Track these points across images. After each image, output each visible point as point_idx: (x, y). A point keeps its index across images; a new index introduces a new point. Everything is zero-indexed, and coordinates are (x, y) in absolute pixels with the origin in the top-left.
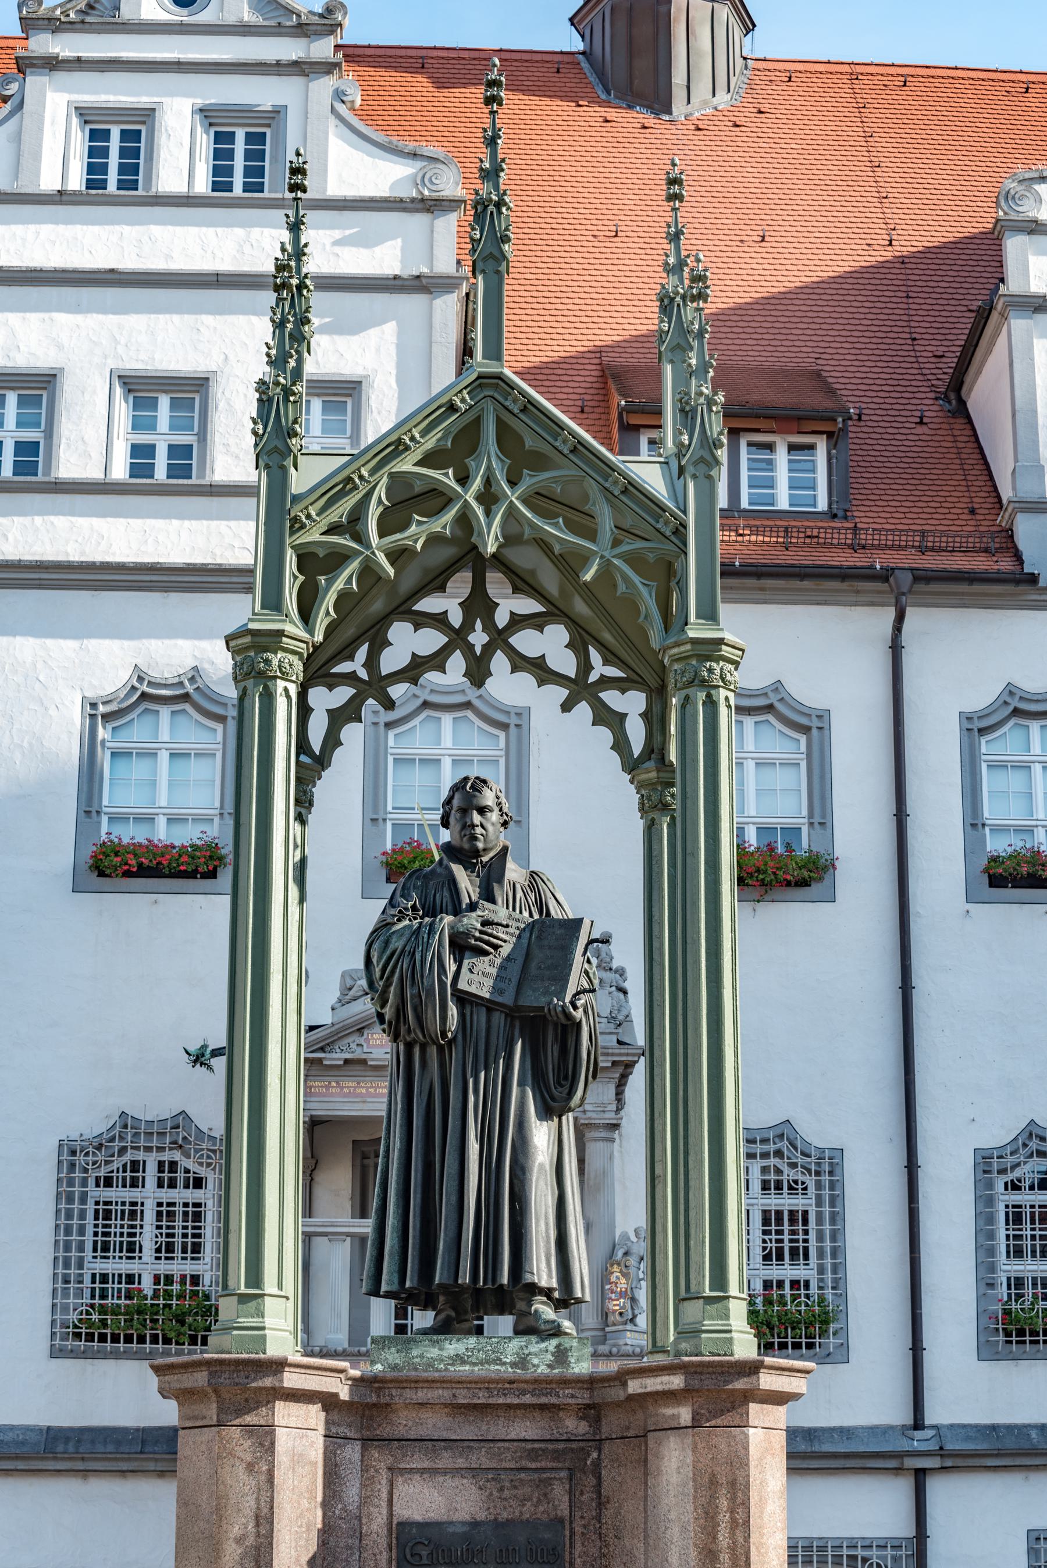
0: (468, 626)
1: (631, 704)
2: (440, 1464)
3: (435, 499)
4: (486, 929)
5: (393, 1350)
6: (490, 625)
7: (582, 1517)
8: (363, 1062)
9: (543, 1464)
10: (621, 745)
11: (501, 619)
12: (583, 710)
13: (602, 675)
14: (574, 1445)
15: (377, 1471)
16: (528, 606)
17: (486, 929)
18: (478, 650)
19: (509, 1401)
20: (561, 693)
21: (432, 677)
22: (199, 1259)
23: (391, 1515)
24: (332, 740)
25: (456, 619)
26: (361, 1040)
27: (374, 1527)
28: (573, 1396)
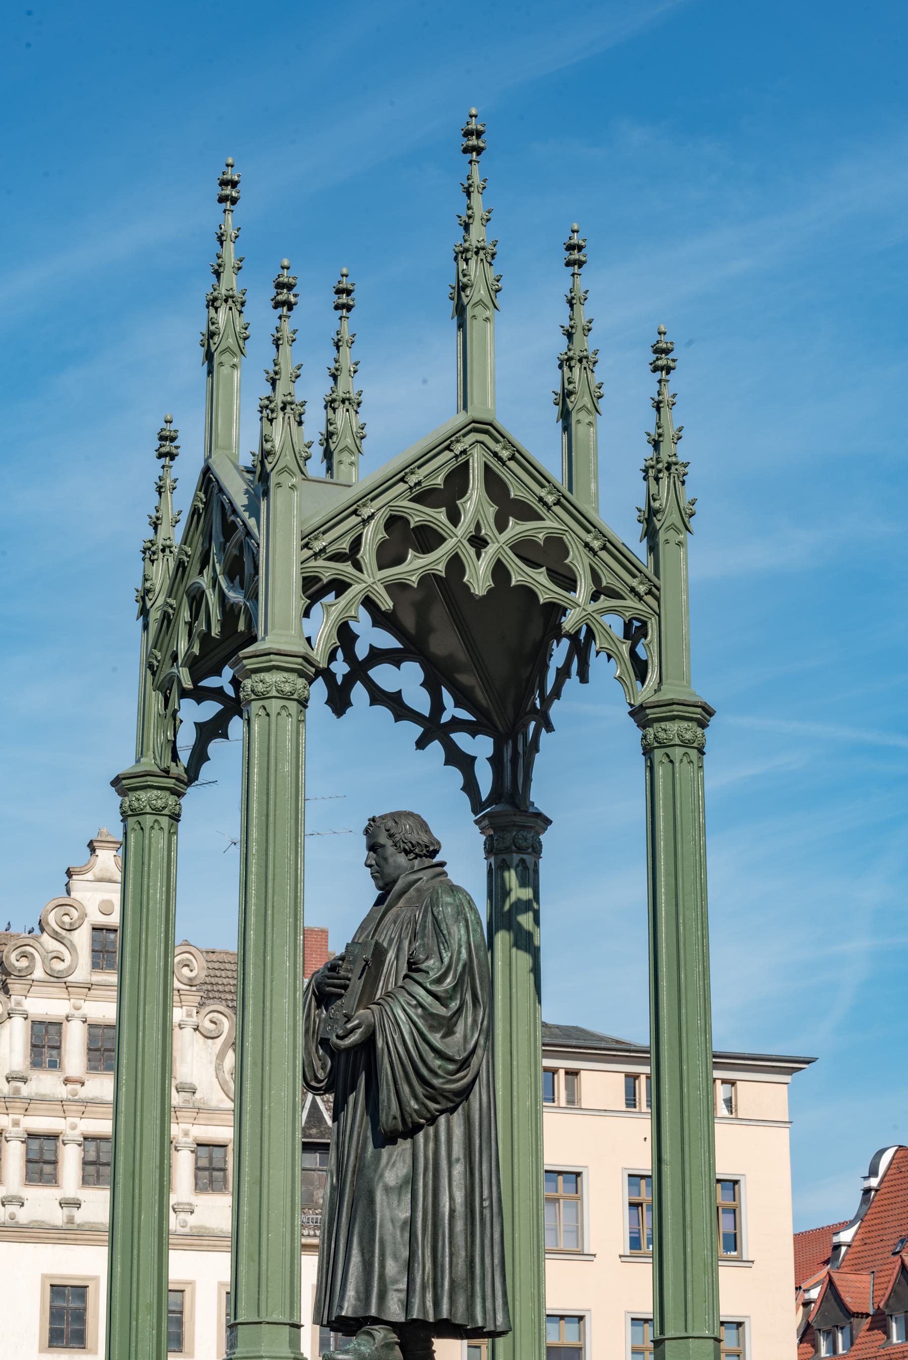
1: (480, 747)
3: (427, 539)
6: (350, 657)
10: (470, 786)
11: (361, 651)
12: (436, 748)
13: (453, 717)
16: (387, 641)
18: (339, 680)
20: (418, 730)
24: (200, 756)
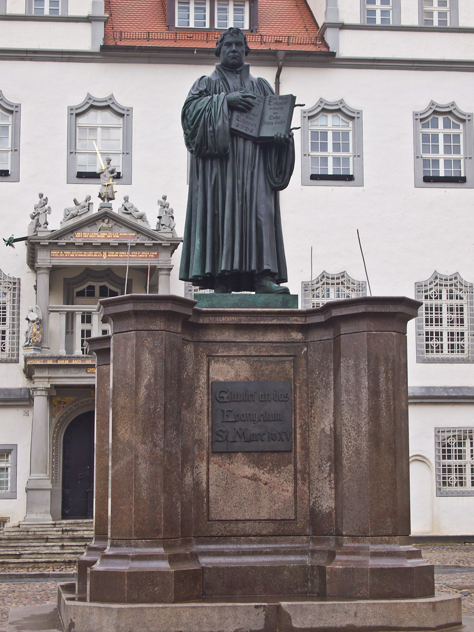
2: (232, 353)
5: (205, 300)
7: (300, 379)
8: (74, 244)
9: (281, 354)
14: (296, 345)
15: (202, 357)
19: (266, 322)
22: (5, 324)
23: (208, 378)
26: (72, 235)
27: (201, 383)
28: (296, 320)
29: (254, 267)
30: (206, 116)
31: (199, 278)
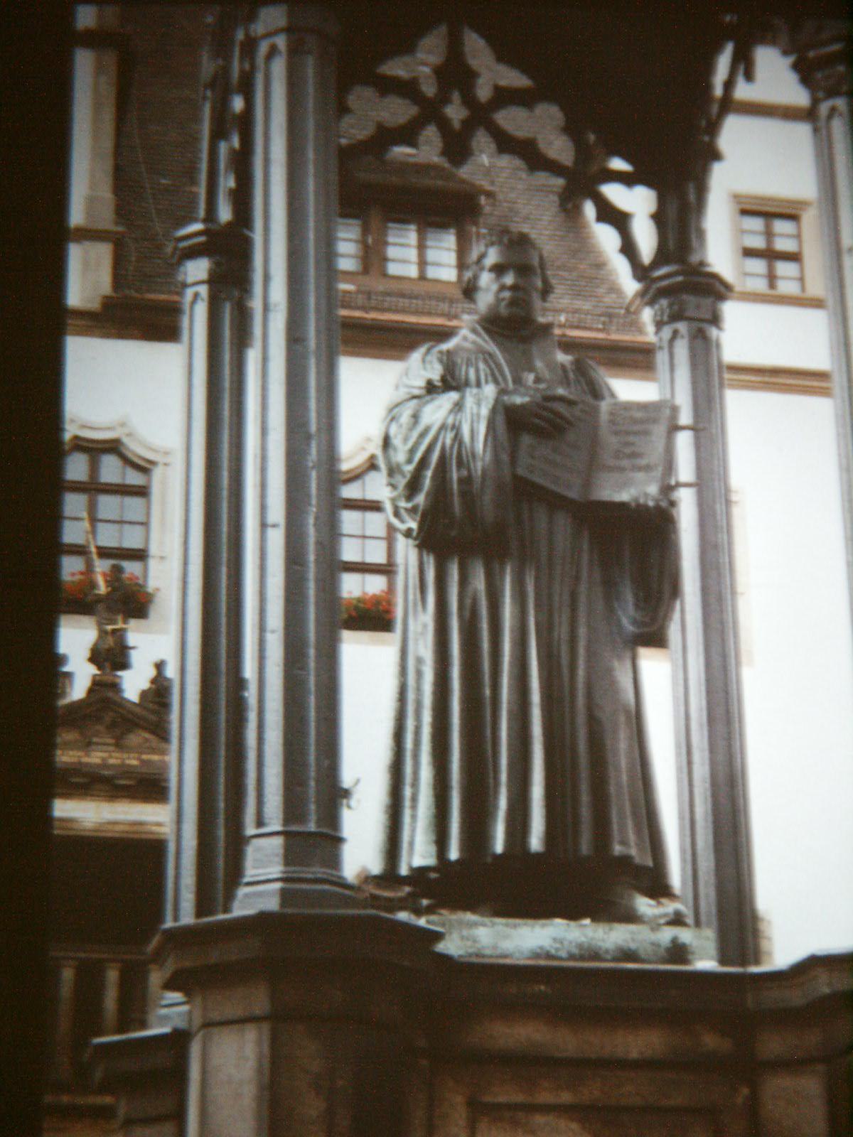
0: (444, 99)
4: (549, 404)
6: (469, 100)
11: (483, 92)
16: (515, 79)
17: (549, 404)
21: (401, 151)
25: (429, 89)
29: (585, 847)
30: (448, 442)
31: (433, 875)
